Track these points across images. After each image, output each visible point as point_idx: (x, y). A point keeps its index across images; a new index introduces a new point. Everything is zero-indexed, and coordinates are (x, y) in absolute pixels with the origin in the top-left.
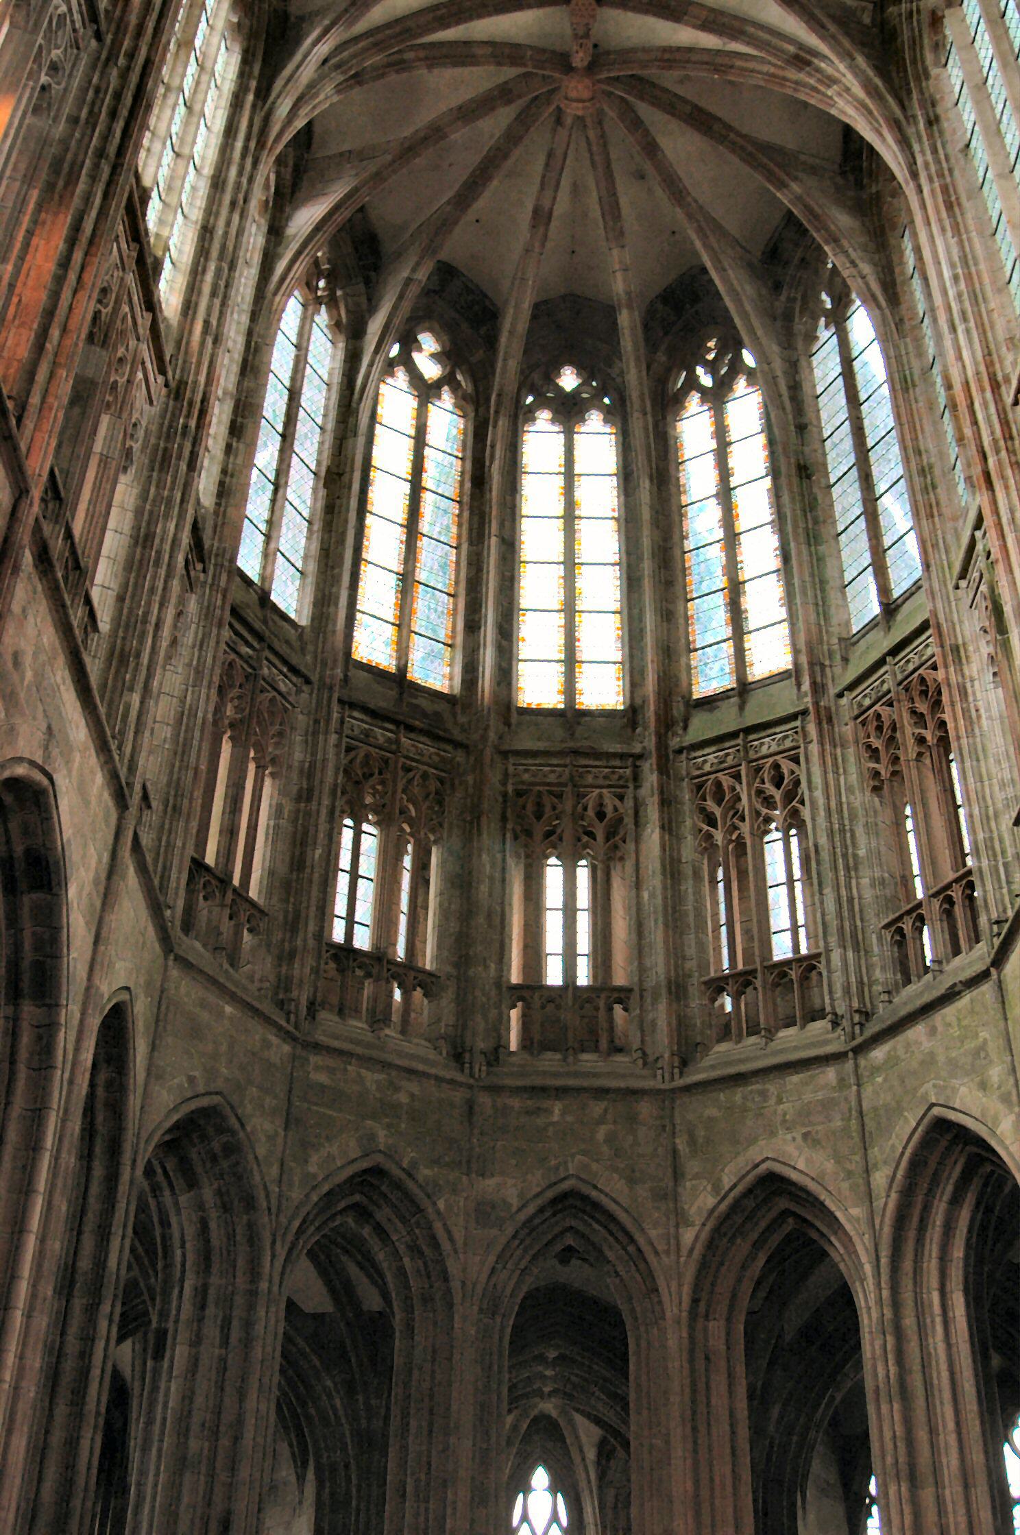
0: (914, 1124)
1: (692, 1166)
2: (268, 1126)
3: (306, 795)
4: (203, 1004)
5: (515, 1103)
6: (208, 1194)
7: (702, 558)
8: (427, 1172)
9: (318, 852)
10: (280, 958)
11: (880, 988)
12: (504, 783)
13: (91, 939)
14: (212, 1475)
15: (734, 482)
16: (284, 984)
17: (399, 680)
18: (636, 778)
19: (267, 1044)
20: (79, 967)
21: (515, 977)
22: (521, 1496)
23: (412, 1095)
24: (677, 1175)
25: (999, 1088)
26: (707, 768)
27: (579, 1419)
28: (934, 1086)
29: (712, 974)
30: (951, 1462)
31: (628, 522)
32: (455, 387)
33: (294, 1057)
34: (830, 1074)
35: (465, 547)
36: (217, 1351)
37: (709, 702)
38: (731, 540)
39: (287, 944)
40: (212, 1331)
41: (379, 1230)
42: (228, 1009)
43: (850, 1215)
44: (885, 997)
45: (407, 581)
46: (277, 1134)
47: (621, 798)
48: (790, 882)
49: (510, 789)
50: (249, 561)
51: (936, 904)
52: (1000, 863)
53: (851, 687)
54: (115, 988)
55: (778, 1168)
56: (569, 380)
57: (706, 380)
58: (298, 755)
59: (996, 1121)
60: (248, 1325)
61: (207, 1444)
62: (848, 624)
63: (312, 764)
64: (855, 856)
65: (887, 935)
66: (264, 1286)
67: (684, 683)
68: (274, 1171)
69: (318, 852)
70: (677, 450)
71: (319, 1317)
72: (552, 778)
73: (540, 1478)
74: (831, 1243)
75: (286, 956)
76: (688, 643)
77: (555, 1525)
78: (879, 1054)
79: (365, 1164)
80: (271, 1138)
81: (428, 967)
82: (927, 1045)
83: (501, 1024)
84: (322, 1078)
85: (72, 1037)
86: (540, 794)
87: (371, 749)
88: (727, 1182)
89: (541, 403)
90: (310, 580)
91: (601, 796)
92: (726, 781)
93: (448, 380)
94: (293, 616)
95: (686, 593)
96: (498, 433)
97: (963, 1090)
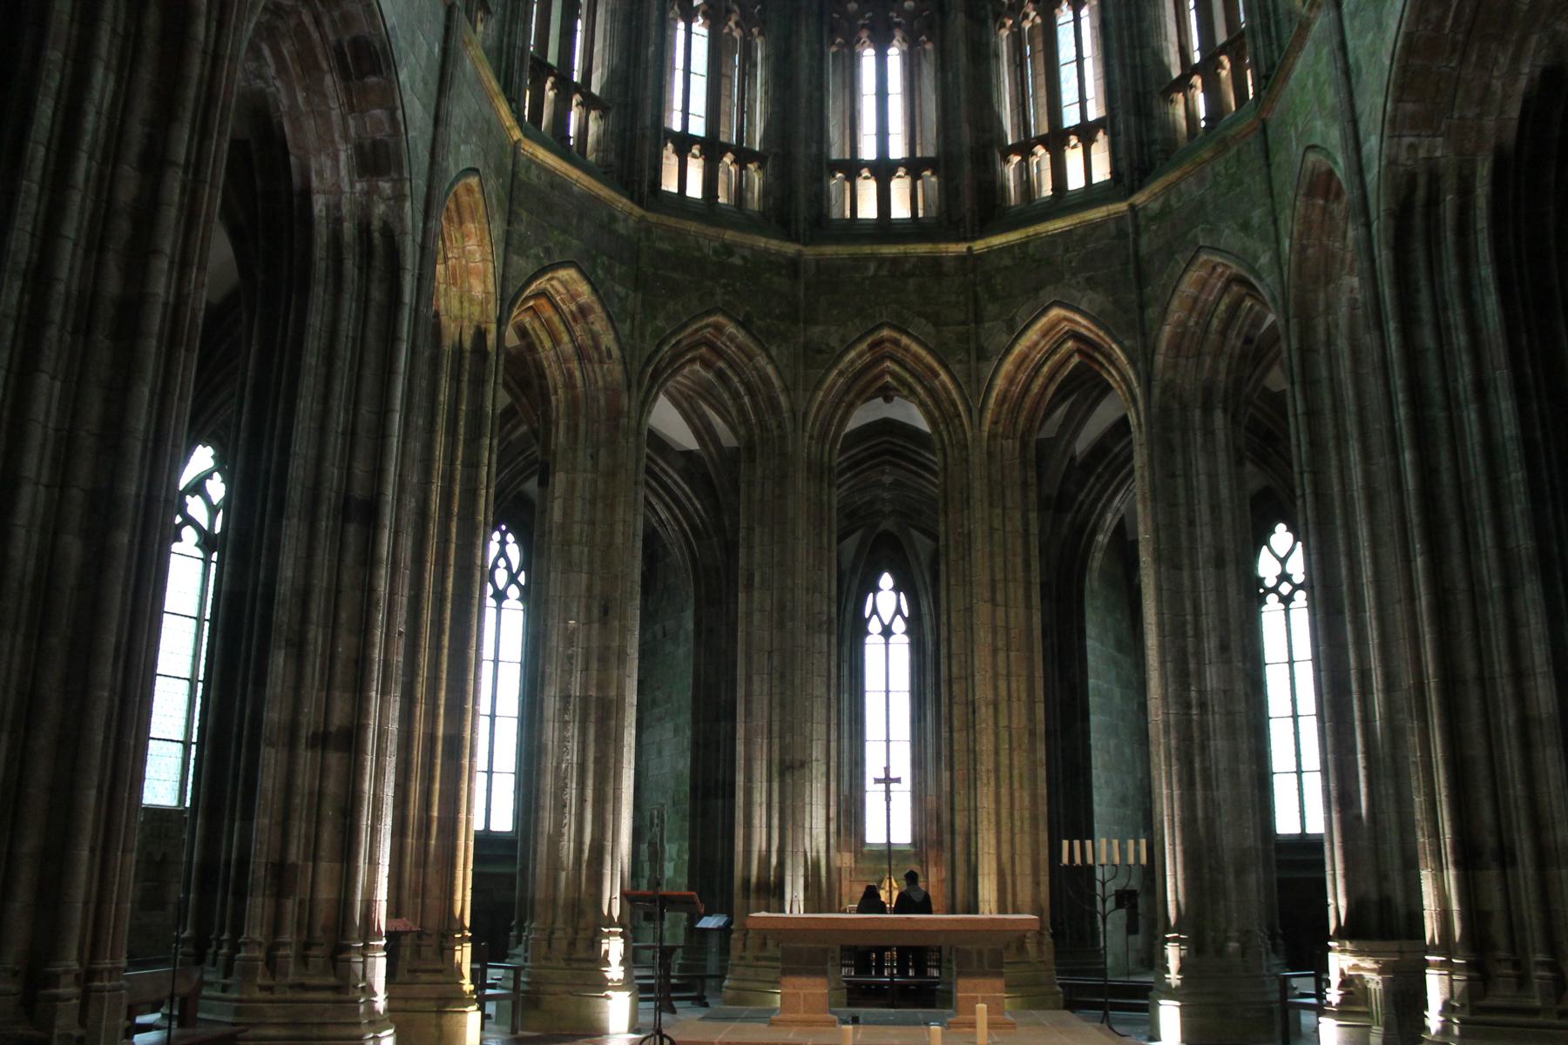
0: (1184, 265)
1: (991, 309)
8: (759, 323)
9: (651, 49)
11: (1158, 147)
13: (431, 122)
14: (591, 573)
20: (420, 148)
21: (835, 155)
22: (871, 595)
23: (744, 258)
24: (978, 319)
25: (1259, 227)
27: (915, 533)
28: (1202, 229)
29: (1010, 143)
36: (589, 476)
39: (628, 133)
41: (720, 375)
46: (627, 295)
48: (1079, 59)
52: (1272, 21)
54: (461, 168)
59: (1256, 258)
61: (586, 549)
71: (688, 454)
73: (886, 581)
74: (1110, 373)
77: (898, 617)
81: (757, 149)
85: (420, 205)
97: (1227, 231)
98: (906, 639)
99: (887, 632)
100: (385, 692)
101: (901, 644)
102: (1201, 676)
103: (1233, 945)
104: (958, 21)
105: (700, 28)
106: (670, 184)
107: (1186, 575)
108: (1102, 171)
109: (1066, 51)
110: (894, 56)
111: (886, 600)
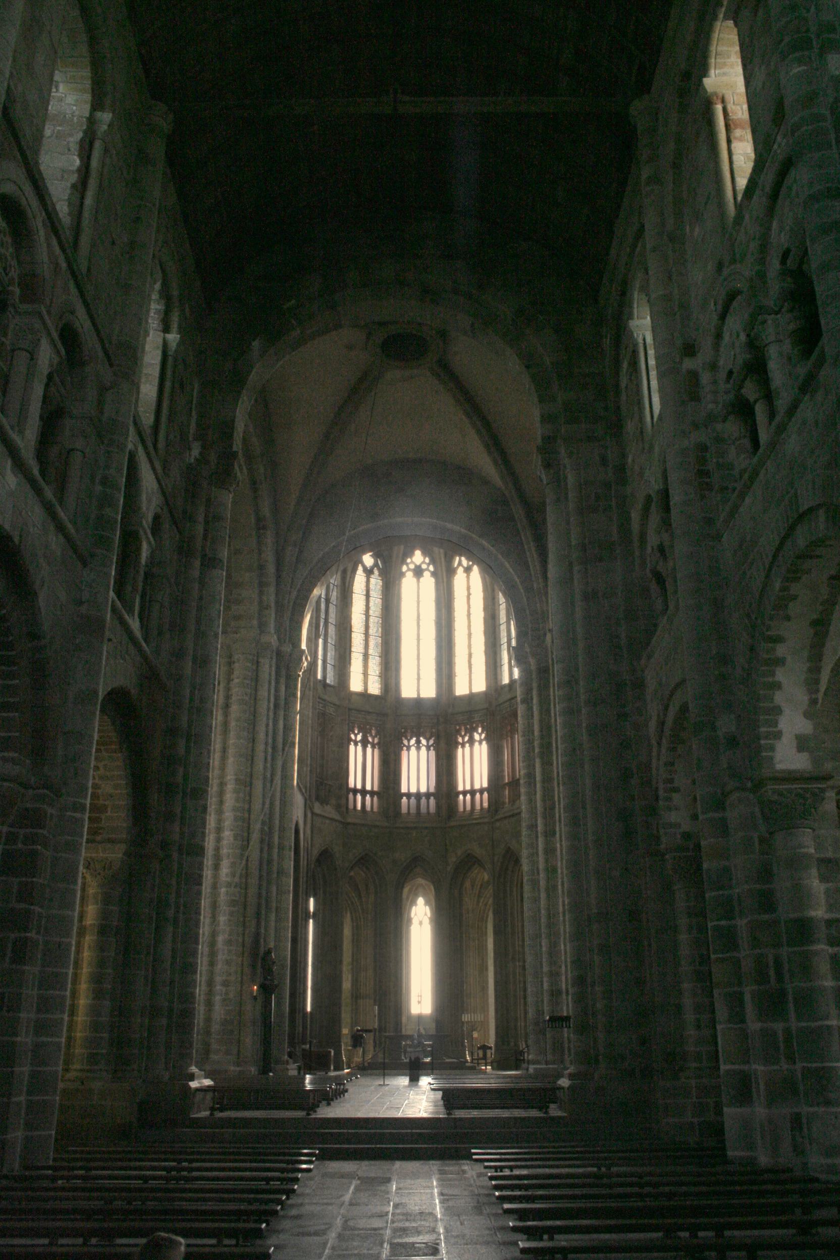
15: (472, 611)
17: (365, 695)
22: (414, 908)
32: (379, 569)
37: (462, 698)
42: (327, 821)
45: (366, 656)
50: (319, 677)
56: (418, 557)
62: (501, 680)
73: (421, 901)
78: (498, 824)
88: (459, 852)
89: (409, 569)
93: (376, 565)
94: (332, 684)
99: (421, 923)
103: (512, 1044)
105: (359, 748)
106: (351, 806)
108: (486, 805)
110: (423, 750)
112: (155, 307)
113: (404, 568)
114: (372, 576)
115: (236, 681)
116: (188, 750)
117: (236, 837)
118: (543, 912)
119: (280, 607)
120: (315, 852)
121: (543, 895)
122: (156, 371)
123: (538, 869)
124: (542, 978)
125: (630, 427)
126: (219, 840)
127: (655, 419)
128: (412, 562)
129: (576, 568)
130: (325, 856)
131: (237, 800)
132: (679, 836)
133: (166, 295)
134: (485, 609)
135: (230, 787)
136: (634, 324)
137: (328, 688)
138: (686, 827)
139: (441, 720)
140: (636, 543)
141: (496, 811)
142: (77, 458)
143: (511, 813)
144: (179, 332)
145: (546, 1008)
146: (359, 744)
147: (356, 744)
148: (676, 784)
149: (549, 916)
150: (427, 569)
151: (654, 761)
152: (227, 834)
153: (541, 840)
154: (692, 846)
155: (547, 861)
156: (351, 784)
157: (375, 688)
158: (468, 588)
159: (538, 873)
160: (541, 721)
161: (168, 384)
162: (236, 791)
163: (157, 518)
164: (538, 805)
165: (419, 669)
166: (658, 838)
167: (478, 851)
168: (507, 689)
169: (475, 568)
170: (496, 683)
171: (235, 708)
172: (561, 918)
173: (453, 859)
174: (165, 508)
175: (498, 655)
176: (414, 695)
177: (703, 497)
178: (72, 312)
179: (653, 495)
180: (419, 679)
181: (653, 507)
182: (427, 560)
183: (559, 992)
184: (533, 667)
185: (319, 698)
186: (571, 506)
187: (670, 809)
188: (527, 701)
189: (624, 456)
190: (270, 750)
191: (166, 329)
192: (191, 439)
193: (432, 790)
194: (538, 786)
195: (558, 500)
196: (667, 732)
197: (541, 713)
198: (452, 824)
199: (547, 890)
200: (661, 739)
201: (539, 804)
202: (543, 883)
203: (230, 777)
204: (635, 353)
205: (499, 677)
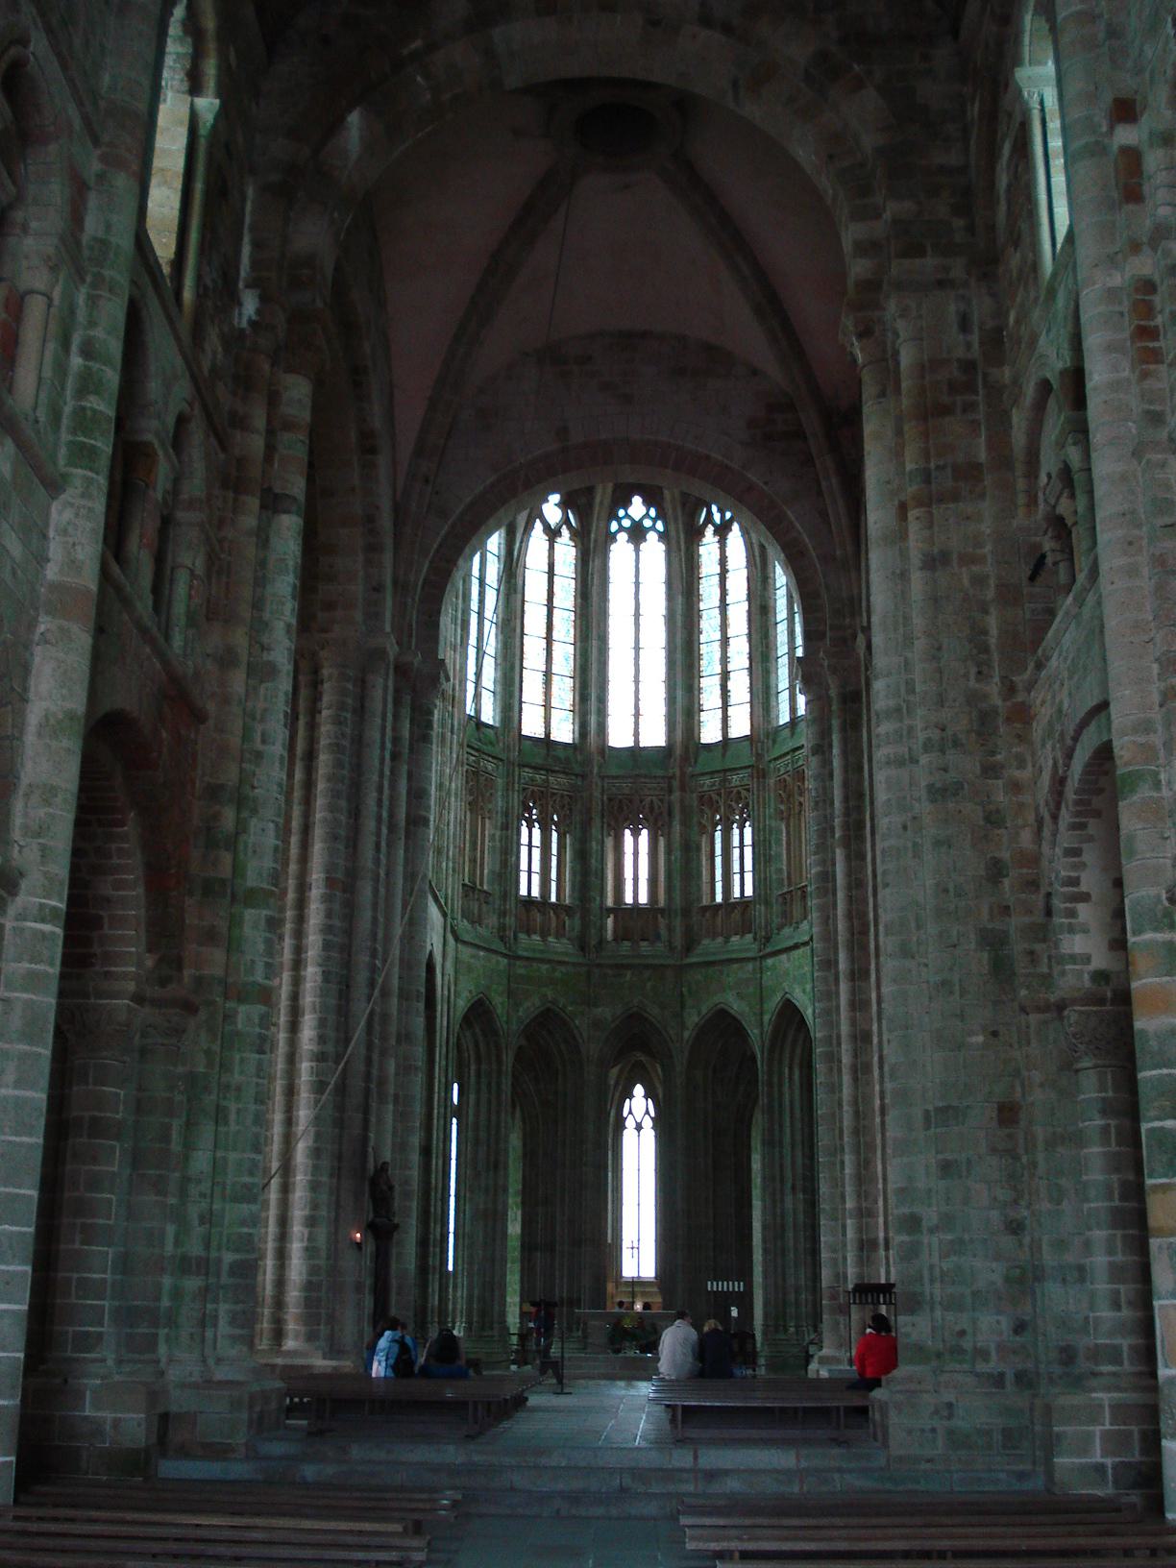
2: (501, 1000)
3: (505, 827)
4: (473, 957)
5: (610, 972)
6: (477, 1030)
7: (709, 649)
10: (499, 915)
12: (602, 794)
14: (488, 1146)
15: (729, 600)
16: (502, 928)
17: (547, 742)
18: (670, 791)
19: (498, 962)
24: (683, 1006)
26: (706, 788)
30: (787, 1139)
31: (670, 619)
33: (509, 965)
34: (750, 966)
35: (578, 644)
38: (725, 641)
40: (484, 1087)
42: (482, 953)
43: (754, 1033)
44: (776, 931)
45: (548, 675)
47: (661, 800)
49: (605, 797)
50: (470, 710)
51: (799, 892)
53: (775, 759)
55: (726, 1007)
56: (637, 507)
57: (717, 517)
58: (500, 804)
59: (806, 1009)
60: (499, 1084)
62: (778, 716)
63: (507, 808)
64: (770, 855)
65: (780, 900)
66: (504, 1068)
67: (696, 735)
68: (505, 1019)
69: (514, 859)
70: (699, 567)
72: (627, 791)
73: (639, 1090)
75: (503, 914)
76: (700, 705)
78: (770, 962)
79: (542, 1009)
80: (502, 1004)
82: (787, 965)
83: (603, 928)
84: (521, 971)
86: (620, 801)
87: (536, 789)
88: (704, 1011)
89: (621, 529)
90: (498, 697)
91: (652, 801)
92: (715, 797)
93: (566, 521)
94: (491, 722)
95: (700, 671)
96: (595, 565)
98: (653, 1133)
99: (639, 1127)
100: (435, 1224)
101: (649, 1134)
102: (782, 1201)
103: (792, 1329)
104: (677, 828)
105: (536, 832)
107: (777, 1149)
109: (736, 842)
110: (645, 833)
111: (639, 1105)
112: (176, 49)
113: (614, 526)
114: (558, 540)
115: (325, 713)
116: (241, 828)
117: (326, 976)
118: (846, 1108)
119: (401, 586)
120: (462, 1004)
121: (846, 1079)
122: (179, 163)
123: (839, 1037)
124: (844, 1218)
125: (1015, 260)
126: (297, 981)
127: (1059, 246)
128: (627, 516)
129: (912, 514)
130: (479, 1012)
131: (329, 914)
132: (1086, 976)
133: (193, 27)
134: (750, 598)
135: (316, 893)
136: (1023, 74)
137: (484, 729)
138: (1100, 960)
139: (676, 783)
140: (1020, 468)
141: (768, 939)
142: (35, 309)
143: (791, 943)
144: (219, 95)
145: (851, 1271)
146: (536, 824)
147: (530, 828)
148: (1083, 888)
149: (857, 1114)
150: (653, 528)
151: (1046, 848)
152: (312, 972)
153: (844, 987)
154: (1109, 994)
155: (853, 1022)
156: (523, 892)
157: (564, 731)
158: (723, 561)
159: (839, 1044)
160: (846, 784)
161: (199, 186)
162: (327, 899)
163: (182, 420)
164: (840, 927)
165: (637, 699)
166: (1047, 979)
167: (736, 1006)
168: (786, 733)
169: (736, 527)
170: (769, 722)
171: (324, 760)
172: (878, 1120)
173: (693, 1019)
174: (197, 405)
175: (773, 676)
176: (630, 743)
177: (1145, 375)
178: (23, 41)
179: (1052, 382)
180: (637, 715)
181: (1052, 404)
182: (653, 512)
183: (873, 1244)
184: (833, 693)
185: (468, 746)
186: (905, 402)
187: (1071, 930)
188: (821, 749)
189: (1001, 313)
190: (384, 830)
191: (195, 87)
192: (241, 285)
193: (662, 902)
194: (840, 895)
195: (883, 394)
196: (1070, 795)
197: (846, 769)
198: (694, 960)
199: (854, 1069)
200: (1058, 807)
201: (841, 925)
202: (846, 1059)
203: (316, 876)
204: (1025, 127)
205: (773, 715)
